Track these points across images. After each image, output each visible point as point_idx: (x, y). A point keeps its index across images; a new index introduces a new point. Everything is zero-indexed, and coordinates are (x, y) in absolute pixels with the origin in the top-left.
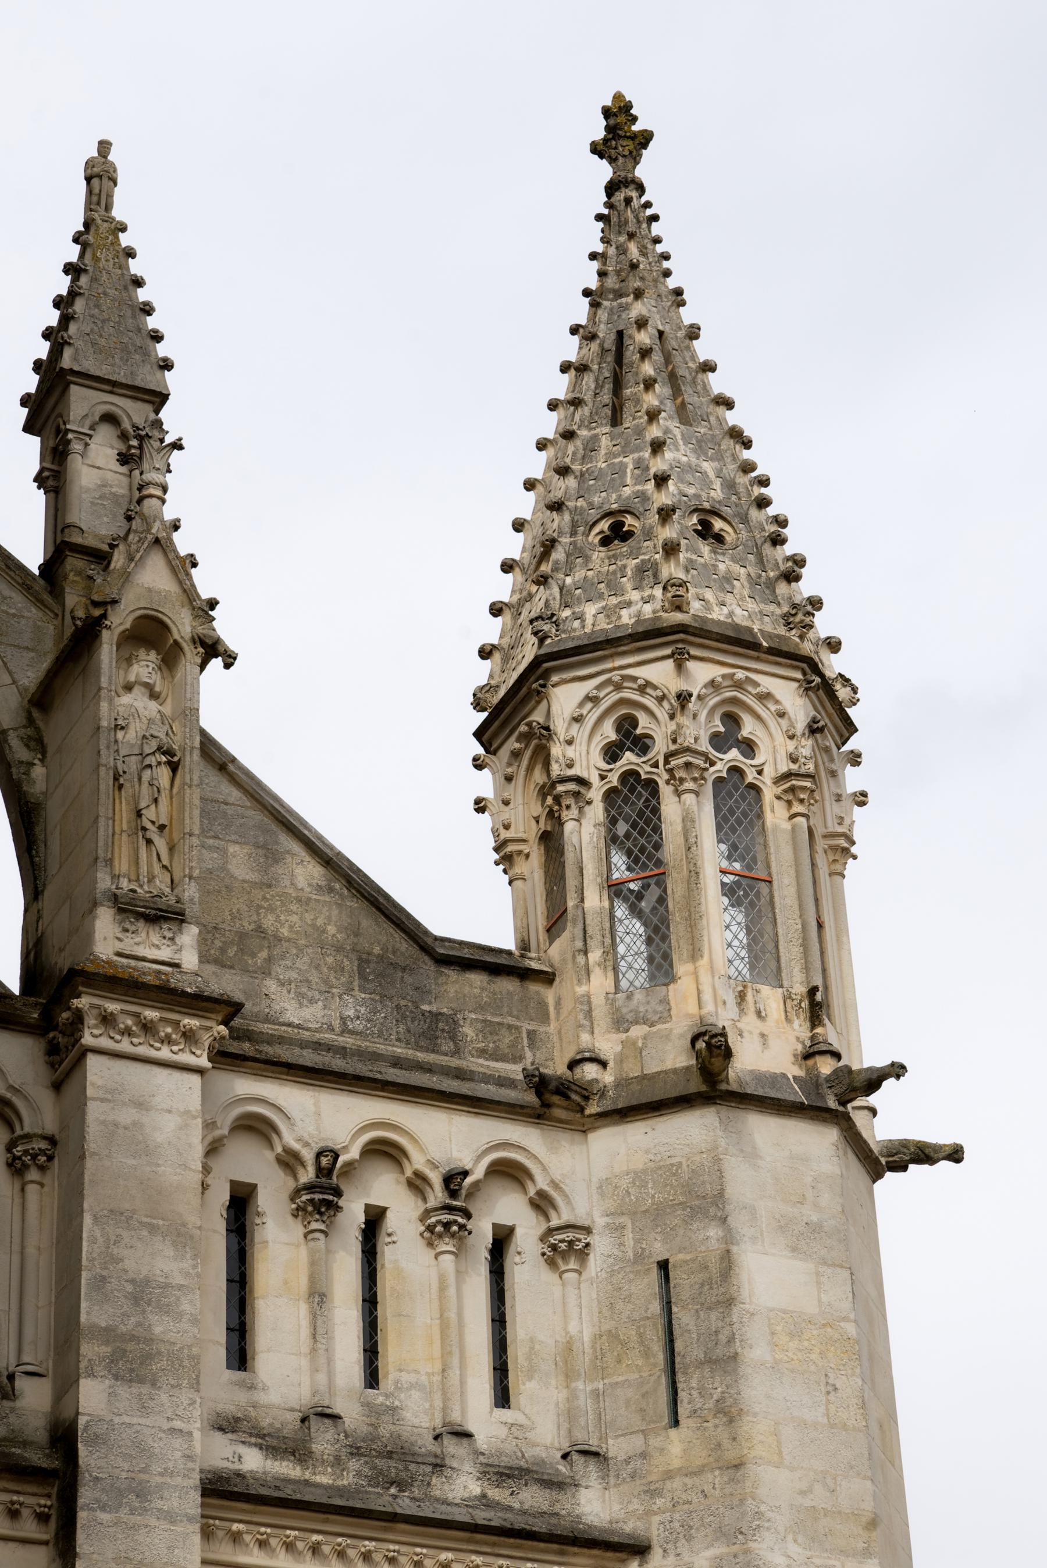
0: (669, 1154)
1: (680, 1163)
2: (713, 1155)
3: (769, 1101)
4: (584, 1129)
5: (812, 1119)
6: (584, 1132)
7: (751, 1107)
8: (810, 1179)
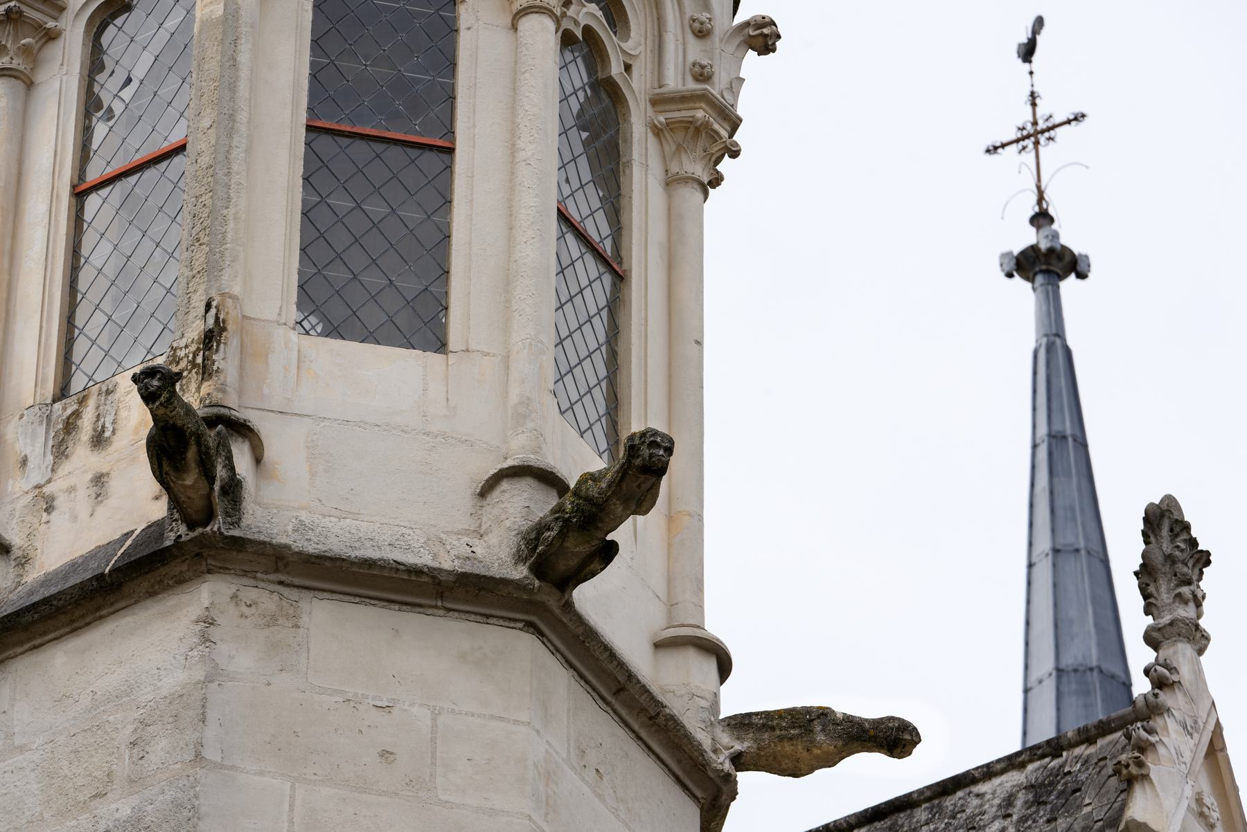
3: (28, 618)
5: (151, 594)
7: (11, 652)
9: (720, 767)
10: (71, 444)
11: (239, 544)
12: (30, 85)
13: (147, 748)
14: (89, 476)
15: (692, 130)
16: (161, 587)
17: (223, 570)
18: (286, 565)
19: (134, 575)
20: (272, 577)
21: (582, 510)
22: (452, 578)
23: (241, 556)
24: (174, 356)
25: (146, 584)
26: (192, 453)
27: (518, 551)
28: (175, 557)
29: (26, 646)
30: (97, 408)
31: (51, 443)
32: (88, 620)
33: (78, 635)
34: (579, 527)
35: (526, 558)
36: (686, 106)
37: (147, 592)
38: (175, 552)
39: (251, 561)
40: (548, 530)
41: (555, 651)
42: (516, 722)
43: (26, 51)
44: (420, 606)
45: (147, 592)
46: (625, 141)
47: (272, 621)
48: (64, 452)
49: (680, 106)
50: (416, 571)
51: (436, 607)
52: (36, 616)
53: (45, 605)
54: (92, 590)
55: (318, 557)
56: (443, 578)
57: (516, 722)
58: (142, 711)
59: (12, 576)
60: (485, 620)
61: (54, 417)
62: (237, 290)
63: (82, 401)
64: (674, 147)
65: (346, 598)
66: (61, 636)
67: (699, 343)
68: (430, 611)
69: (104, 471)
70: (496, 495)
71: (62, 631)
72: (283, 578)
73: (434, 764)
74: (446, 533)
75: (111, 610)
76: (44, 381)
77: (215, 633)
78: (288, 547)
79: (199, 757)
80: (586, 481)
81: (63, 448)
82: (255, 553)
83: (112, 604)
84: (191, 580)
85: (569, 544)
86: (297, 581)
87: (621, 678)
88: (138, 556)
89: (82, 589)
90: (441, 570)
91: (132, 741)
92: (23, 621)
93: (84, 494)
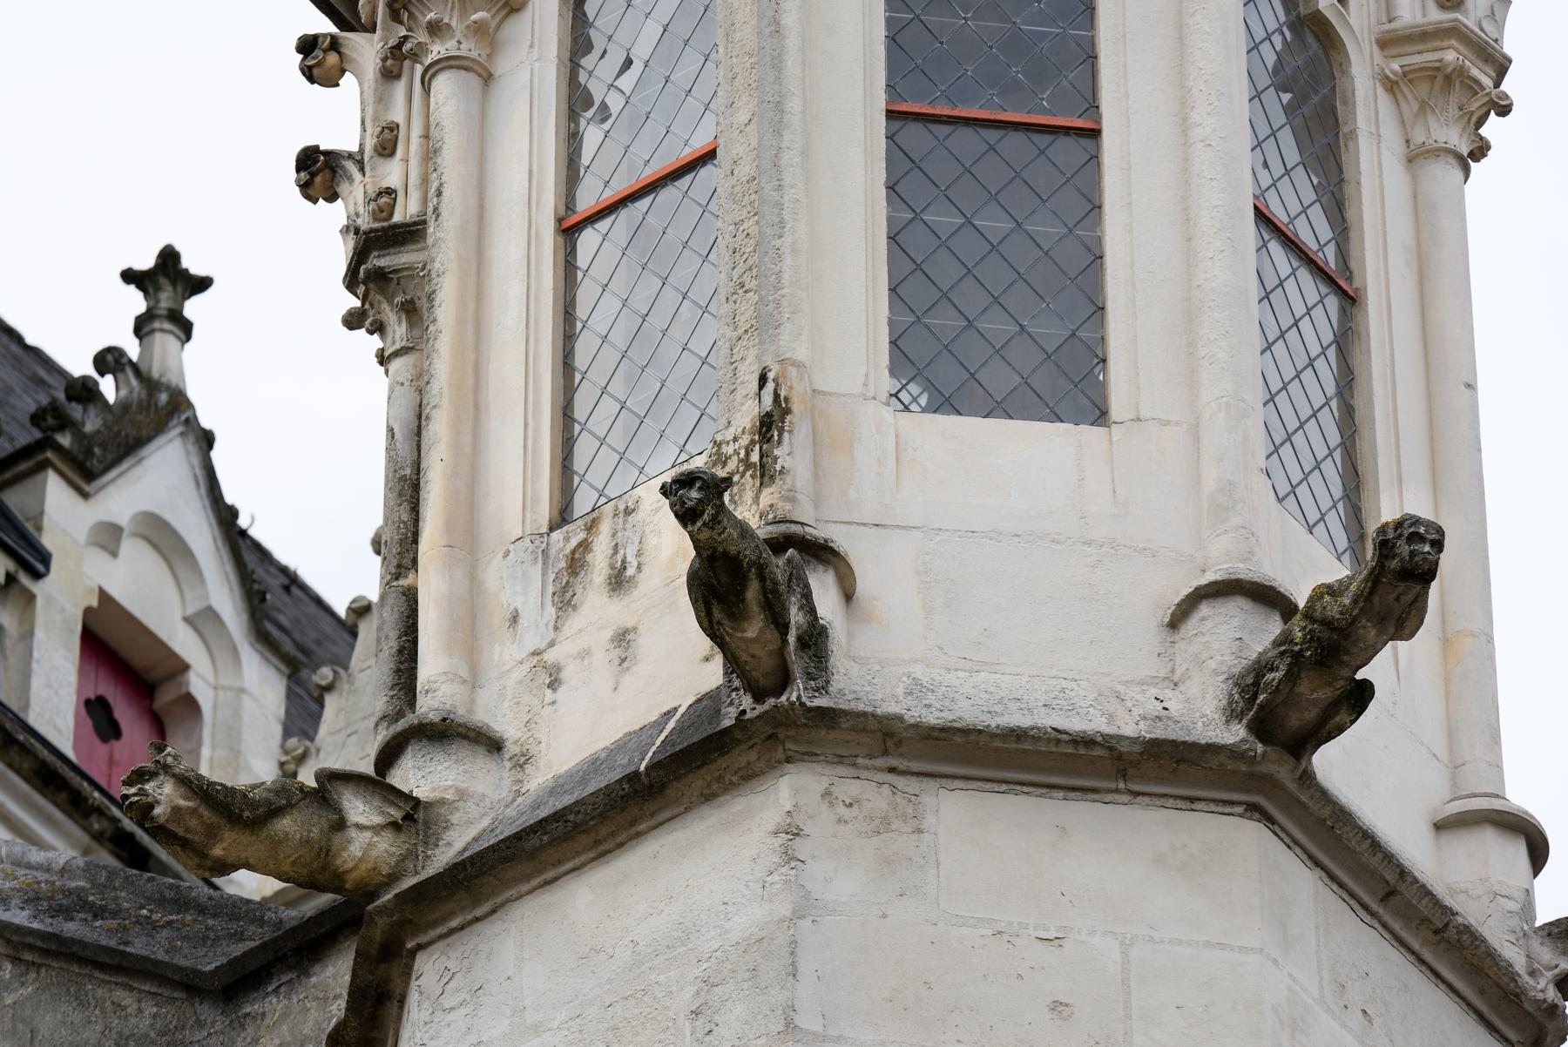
3: (534, 841)
5: (708, 797)
7: (513, 892)
9: (1540, 996)
10: (579, 590)
11: (828, 717)
12: (487, 78)
13: (716, 1018)
14: (609, 634)
15: (1440, 79)
16: (721, 785)
17: (809, 756)
18: (899, 744)
19: (682, 772)
20: (879, 762)
21: (1319, 638)
22: (1137, 748)
23: (833, 735)
24: (719, 453)
25: (700, 782)
26: (753, 592)
27: (1230, 703)
28: (739, 742)
29: (534, 882)
30: (614, 535)
31: (550, 589)
32: (619, 839)
33: (608, 862)
34: (1315, 664)
35: (1242, 712)
36: (1430, 45)
37: (702, 795)
38: (738, 734)
39: (848, 742)
40: (1272, 670)
41: (1293, 843)
42: (1243, 949)
43: (479, 29)
44: (1094, 790)
45: (702, 795)
46: (1345, 103)
47: (883, 825)
48: (569, 602)
49: (1421, 47)
50: (1085, 741)
51: (1117, 791)
52: (545, 838)
53: (558, 822)
54: (622, 797)
55: (943, 729)
56: (1124, 748)
57: (1243, 949)
58: (705, 965)
59: (507, 782)
60: (1188, 805)
61: (553, 552)
62: (801, 354)
63: (591, 527)
64: (1415, 106)
65: (988, 786)
66: (584, 865)
67: (1471, 386)
68: (1109, 797)
69: (630, 625)
70: (1192, 623)
71: (583, 858)
72: (894, 762)
73: (1128, 1017)
74: (1125, 683)
75: (652, 823)
76: (536, 500)
77: (802, 848)
78: (900, 718)
79: (790, 1026)
80: (1322, 597)
81: (568, 595)
82: (853, 729)
83: (653, 815)
84: (764, 773)
85: (1303, 688)
86: (915, 766)
87: (1391, 877)
88: (686, 744)
89: (609, 795)
90: (1120, 738)
91: (693, 1009)
92: (528, 845)
93: (602, 659)
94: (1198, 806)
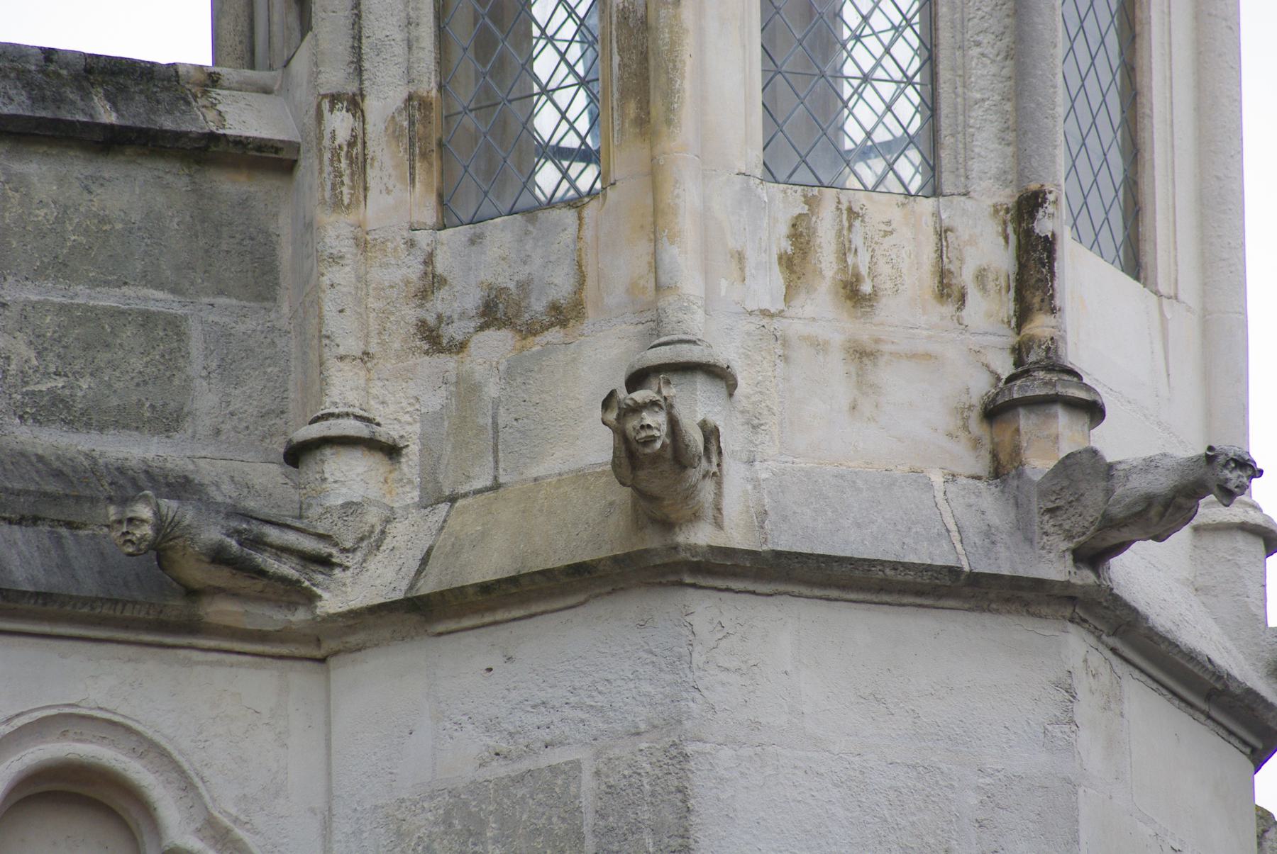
0: (545, 735)
1: (576, 765)
2: (667, 741)
4: (318, 654)
6: (322, 660)
7: (796, 589)
8: (973, 799)
29: (817, 592)
56: (1233, 687)
60: (1225, 734)
68: (1197, 715)
91: (979, 818)
94: (1232, 739)
